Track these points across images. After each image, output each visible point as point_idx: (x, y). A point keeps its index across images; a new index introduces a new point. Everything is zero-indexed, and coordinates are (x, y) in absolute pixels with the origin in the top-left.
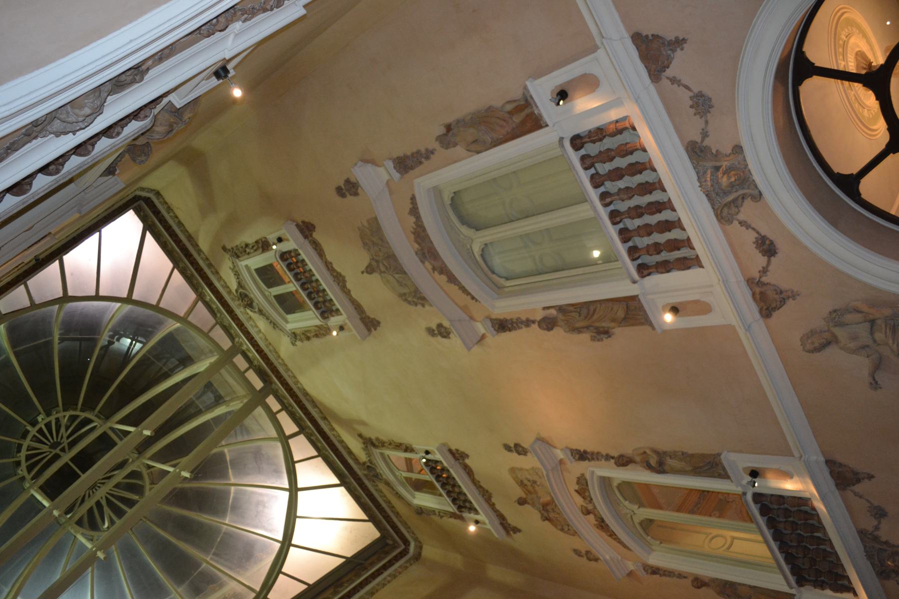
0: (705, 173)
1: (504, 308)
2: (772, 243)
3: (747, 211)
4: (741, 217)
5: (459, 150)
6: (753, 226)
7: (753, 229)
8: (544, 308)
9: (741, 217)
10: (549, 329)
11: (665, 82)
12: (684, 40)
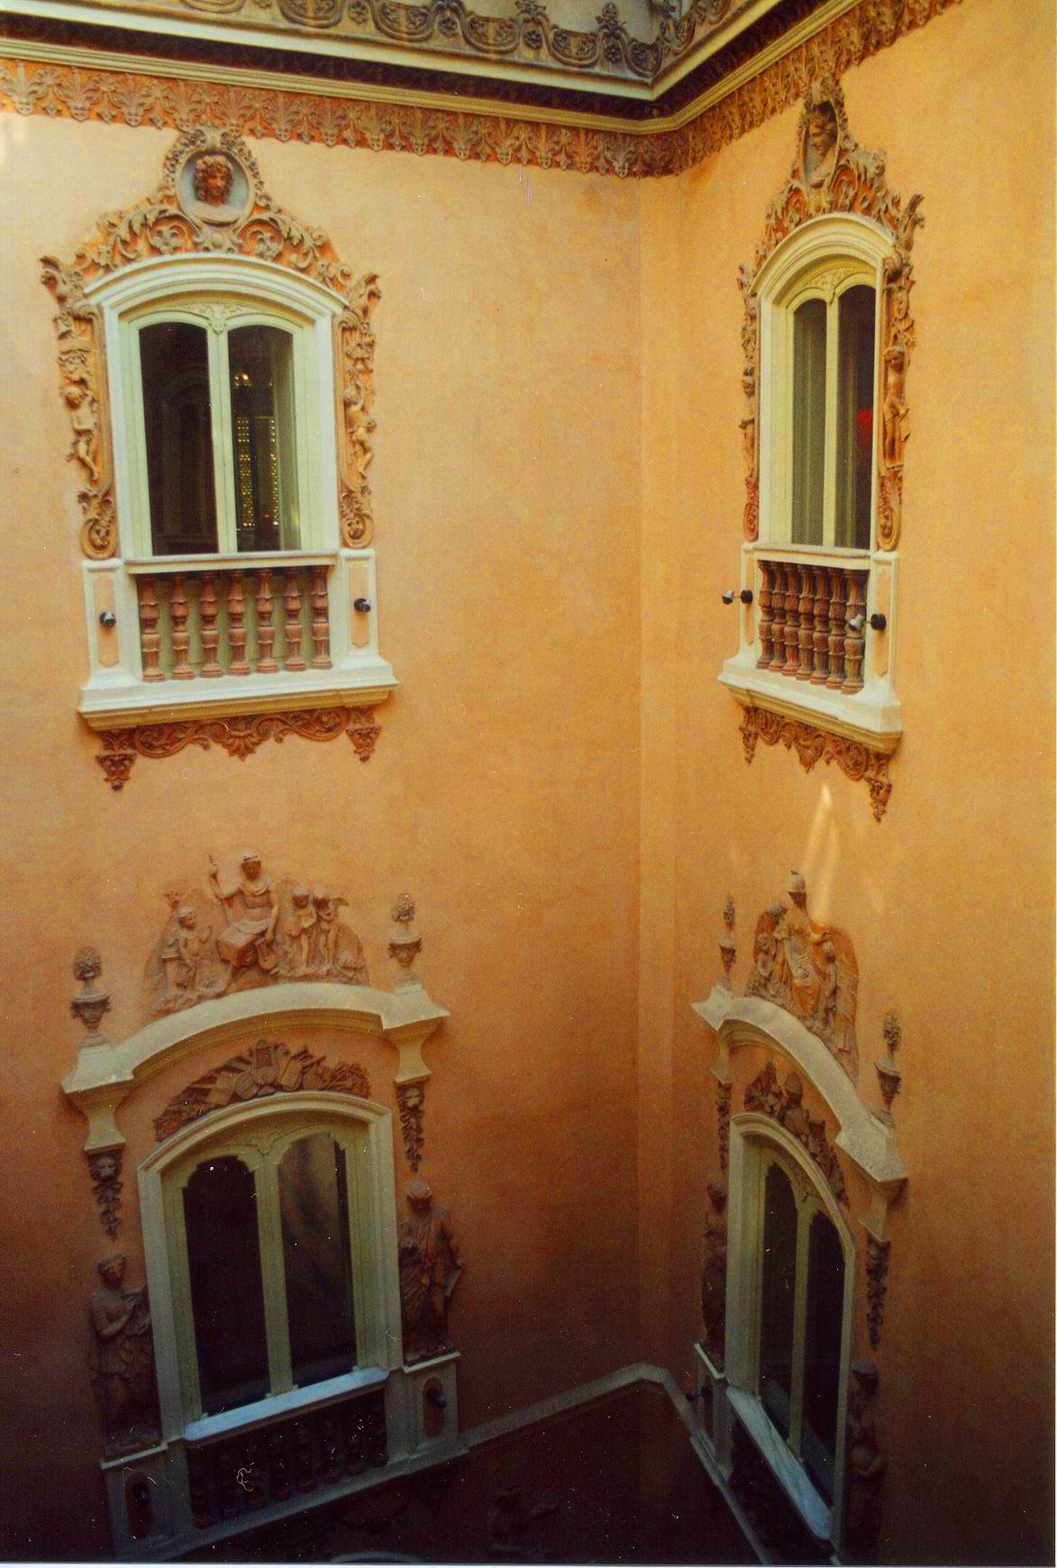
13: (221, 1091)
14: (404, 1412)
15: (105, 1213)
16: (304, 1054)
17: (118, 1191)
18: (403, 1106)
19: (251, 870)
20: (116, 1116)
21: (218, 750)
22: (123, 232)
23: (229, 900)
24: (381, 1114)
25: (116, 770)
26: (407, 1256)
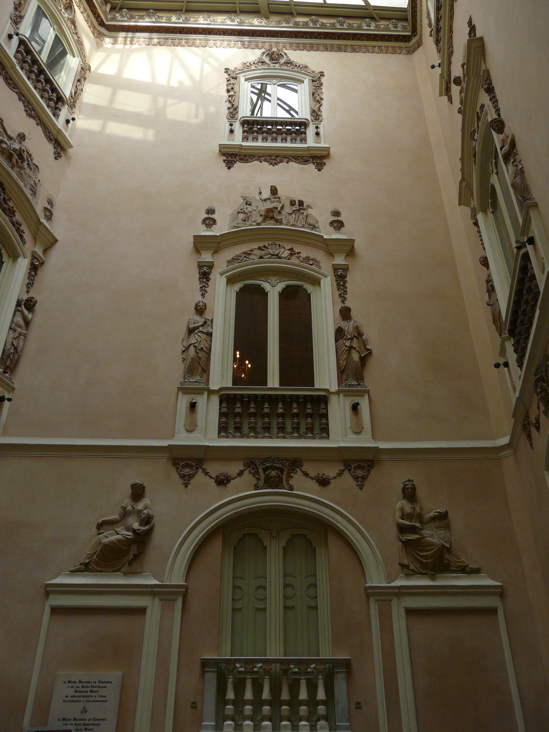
0: (283, 465)
2: (225, 485)
7: (236, 477)
11: (342, 468)
12: (361, 488)
13: (256, 255)
14: (338, 411)
15: (201, 287)
16: (291, 249)
17: (208, 281)
18: (336, 276)
19: (274, 191)
20: (212, 254)
21: (265, 164)
22: (248, 64)
23: (265, 200)
24: (326, 277)
25: (229, 165)
26: (339, 333)
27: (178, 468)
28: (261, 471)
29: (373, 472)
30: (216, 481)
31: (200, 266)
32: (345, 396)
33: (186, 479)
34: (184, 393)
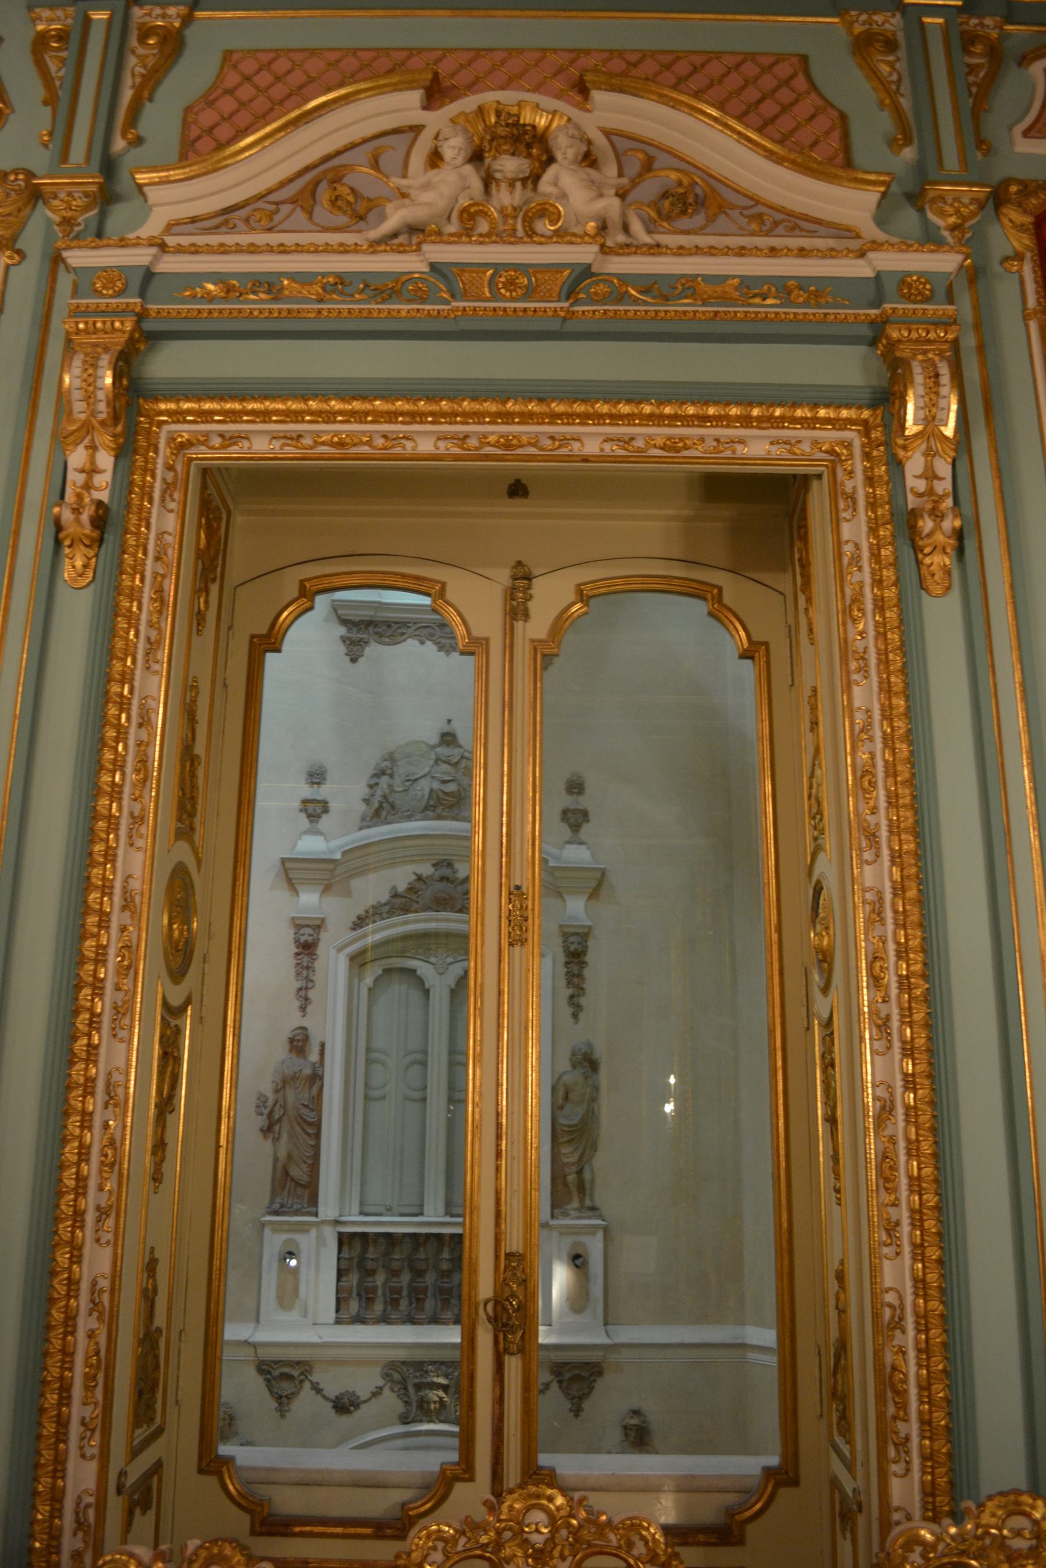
1: (333, 964)
2: (348, 1412)
3: (391, 1401)
4: (387, 1391)
5: (564, 1065)
6: (374, 1400)
7: (369, 1399)
8: (323, 1046)
9: (387, 1391)
10: (292, 1040)
12: (577, 1415)
27: (269, 1381)
28: (411, 1390)
29: (600, 1384)
30: (335, 1407)
31: (298, 925)
32: (561, 1234)
33: (283, 1401)
34: (274, 1231)
